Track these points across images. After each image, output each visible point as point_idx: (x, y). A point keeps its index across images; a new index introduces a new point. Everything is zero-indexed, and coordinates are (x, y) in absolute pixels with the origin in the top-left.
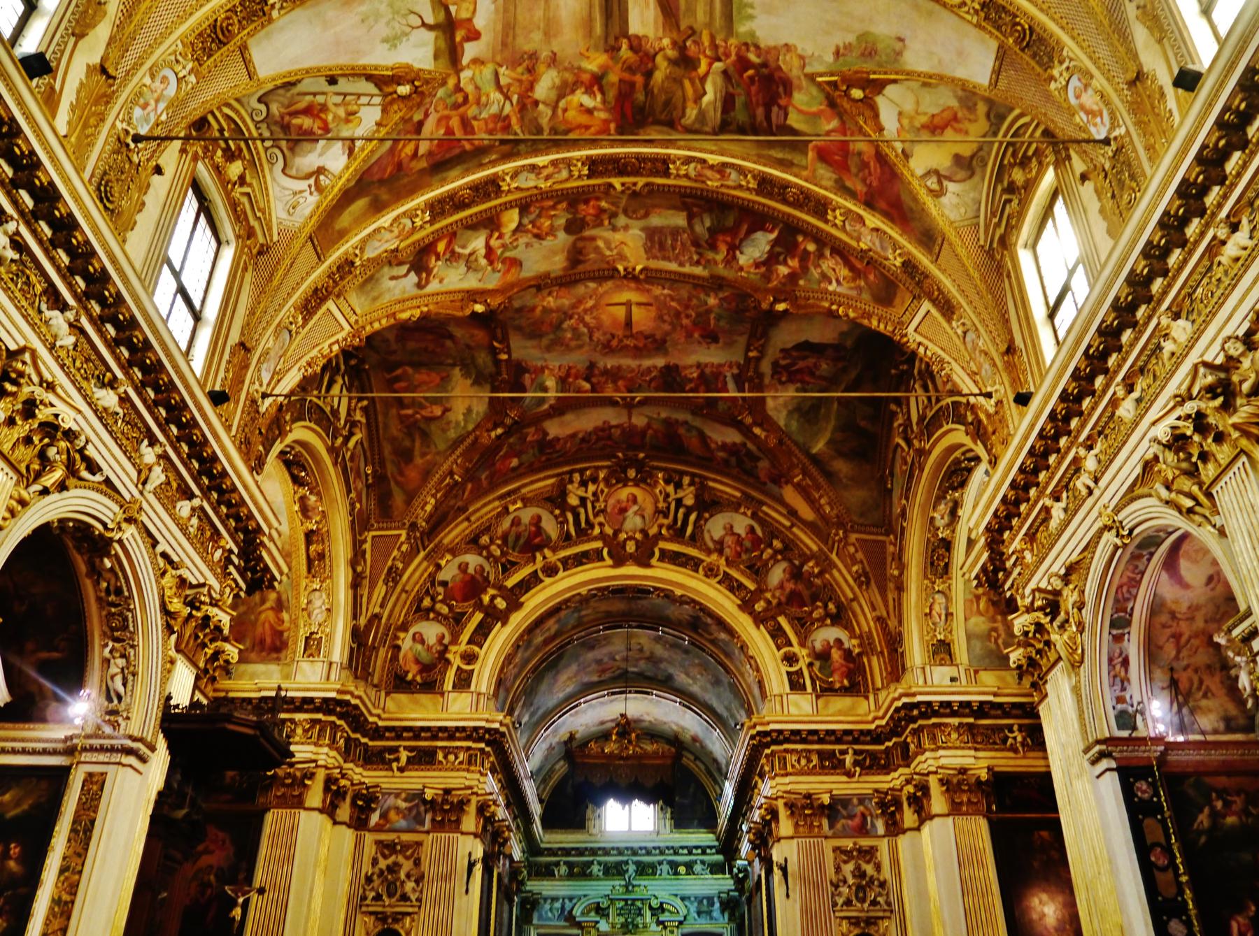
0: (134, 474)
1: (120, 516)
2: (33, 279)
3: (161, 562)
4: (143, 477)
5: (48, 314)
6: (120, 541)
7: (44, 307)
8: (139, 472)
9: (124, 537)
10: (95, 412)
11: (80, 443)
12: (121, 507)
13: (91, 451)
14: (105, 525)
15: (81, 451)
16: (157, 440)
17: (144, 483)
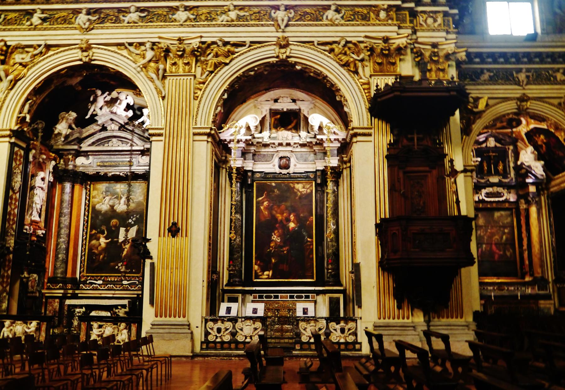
0: (273, 29)
1: (277, 50)
2: (160, 12)
3: (327, 48)
4: (276, 26)
5: (174, 17)
6: (288, 57)
7: (170, 16)
8: (273, 25)
9: (288, 54)
10: (224, 26)
11: (220, 43)
12: (274, 45)
13: (233, 40)
14: (273, 57)
15: (226, 44)
16: (278, 6)
17: (280, 28)
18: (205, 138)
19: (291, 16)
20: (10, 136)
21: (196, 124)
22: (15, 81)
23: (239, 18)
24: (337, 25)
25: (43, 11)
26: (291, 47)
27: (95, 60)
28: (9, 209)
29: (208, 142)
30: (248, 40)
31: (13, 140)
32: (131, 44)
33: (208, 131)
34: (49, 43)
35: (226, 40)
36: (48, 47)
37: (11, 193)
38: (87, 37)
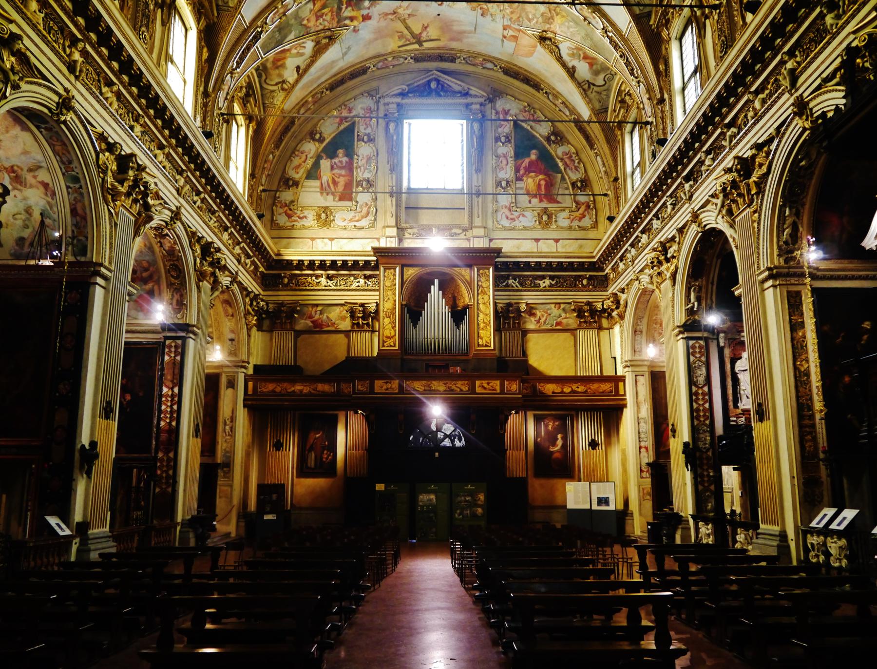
18: (770, 283)
19: (798, 59)
20: (680, 332)
21: (759, 268)
22: (674, 276)
23: (764, 101)
24: (838, 33)
25: (671, 196)
26: (811, 105)
27: (705, 226)
28: (695, 406)
29: (774, 286)
30: (772, 130)
31: (686, 335)
32: (712, 196)
33: (767, 273)
34: (680, 226)
35: (760, 141)
36: (681, 231)
37: (694, 389)
38: (692, 206)
